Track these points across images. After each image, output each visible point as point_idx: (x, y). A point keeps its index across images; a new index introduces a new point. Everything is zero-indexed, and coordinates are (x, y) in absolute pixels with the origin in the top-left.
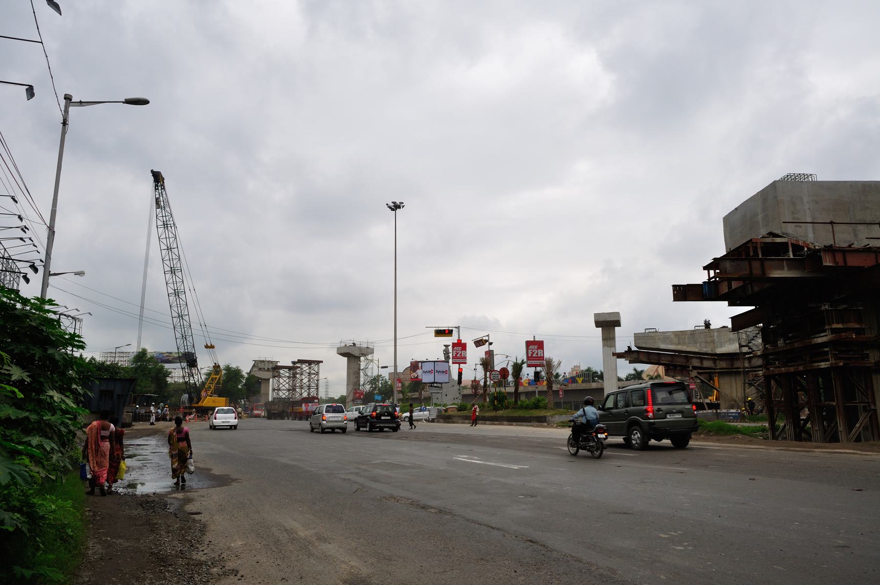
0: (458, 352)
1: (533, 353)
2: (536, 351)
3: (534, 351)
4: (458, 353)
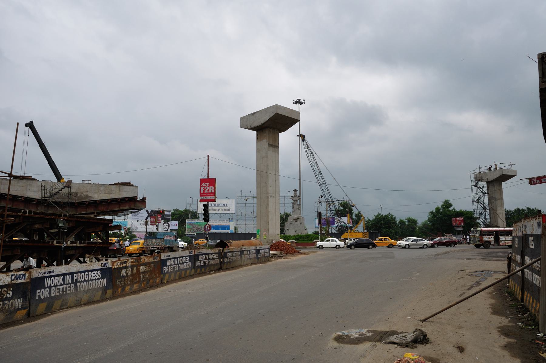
0: (205, 188)
4: (205, 190)
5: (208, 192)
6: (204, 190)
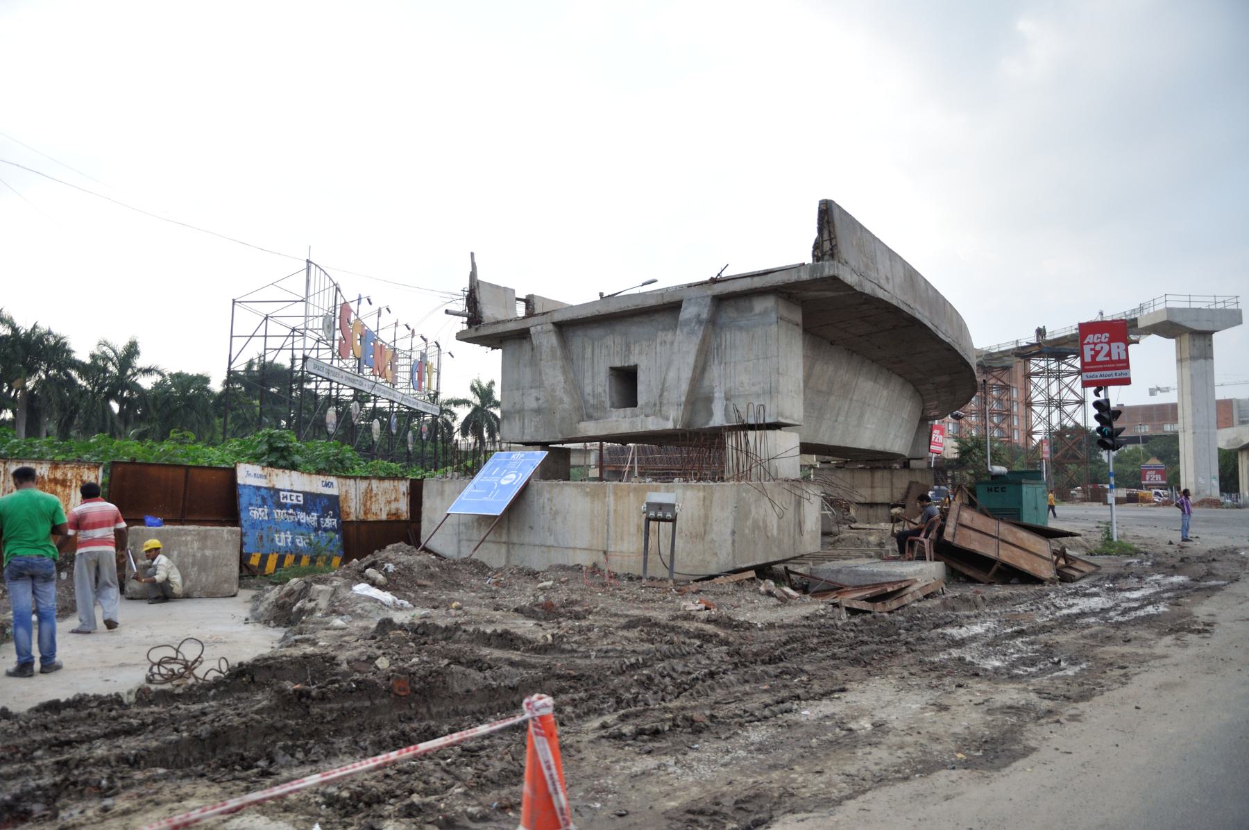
1: (1097, 353)
2: (1106, 347)
3: (1098, 348)
5: (1108, 359)
6: (1093, 353)
